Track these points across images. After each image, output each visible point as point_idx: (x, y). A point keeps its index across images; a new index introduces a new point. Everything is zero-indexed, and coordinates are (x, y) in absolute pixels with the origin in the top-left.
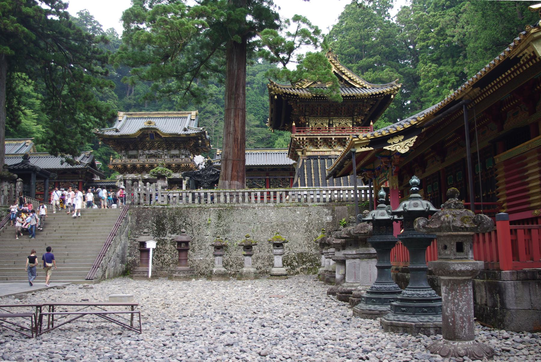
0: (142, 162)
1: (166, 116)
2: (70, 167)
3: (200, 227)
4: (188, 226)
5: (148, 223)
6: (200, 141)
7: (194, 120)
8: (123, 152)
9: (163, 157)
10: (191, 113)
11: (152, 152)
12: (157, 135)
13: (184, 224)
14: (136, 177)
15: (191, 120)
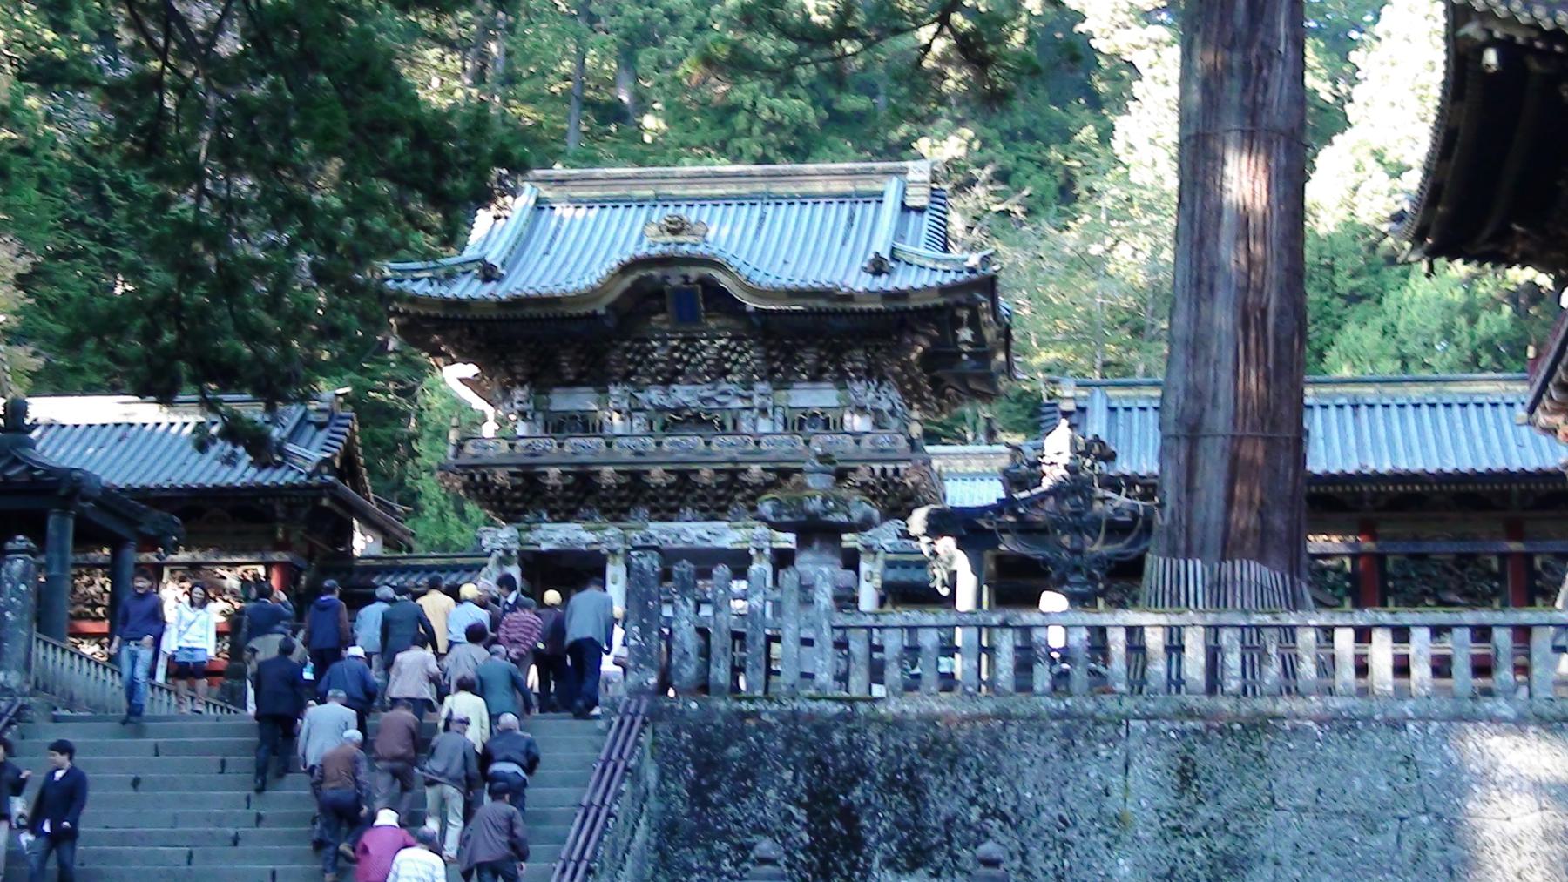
0: (627, 456)
1: (760, 187)
2: (243, 473)
3: (1073, 834)
4: (995, 824)
5: (762, 803)
6: (966, 334)
7: (920, 210)
9: (745, 426)
10: (902, 172)
11: (683, 394)
12: (717, 299)
13: (975, 814)
14: (589, 537)
15: (905, 208)
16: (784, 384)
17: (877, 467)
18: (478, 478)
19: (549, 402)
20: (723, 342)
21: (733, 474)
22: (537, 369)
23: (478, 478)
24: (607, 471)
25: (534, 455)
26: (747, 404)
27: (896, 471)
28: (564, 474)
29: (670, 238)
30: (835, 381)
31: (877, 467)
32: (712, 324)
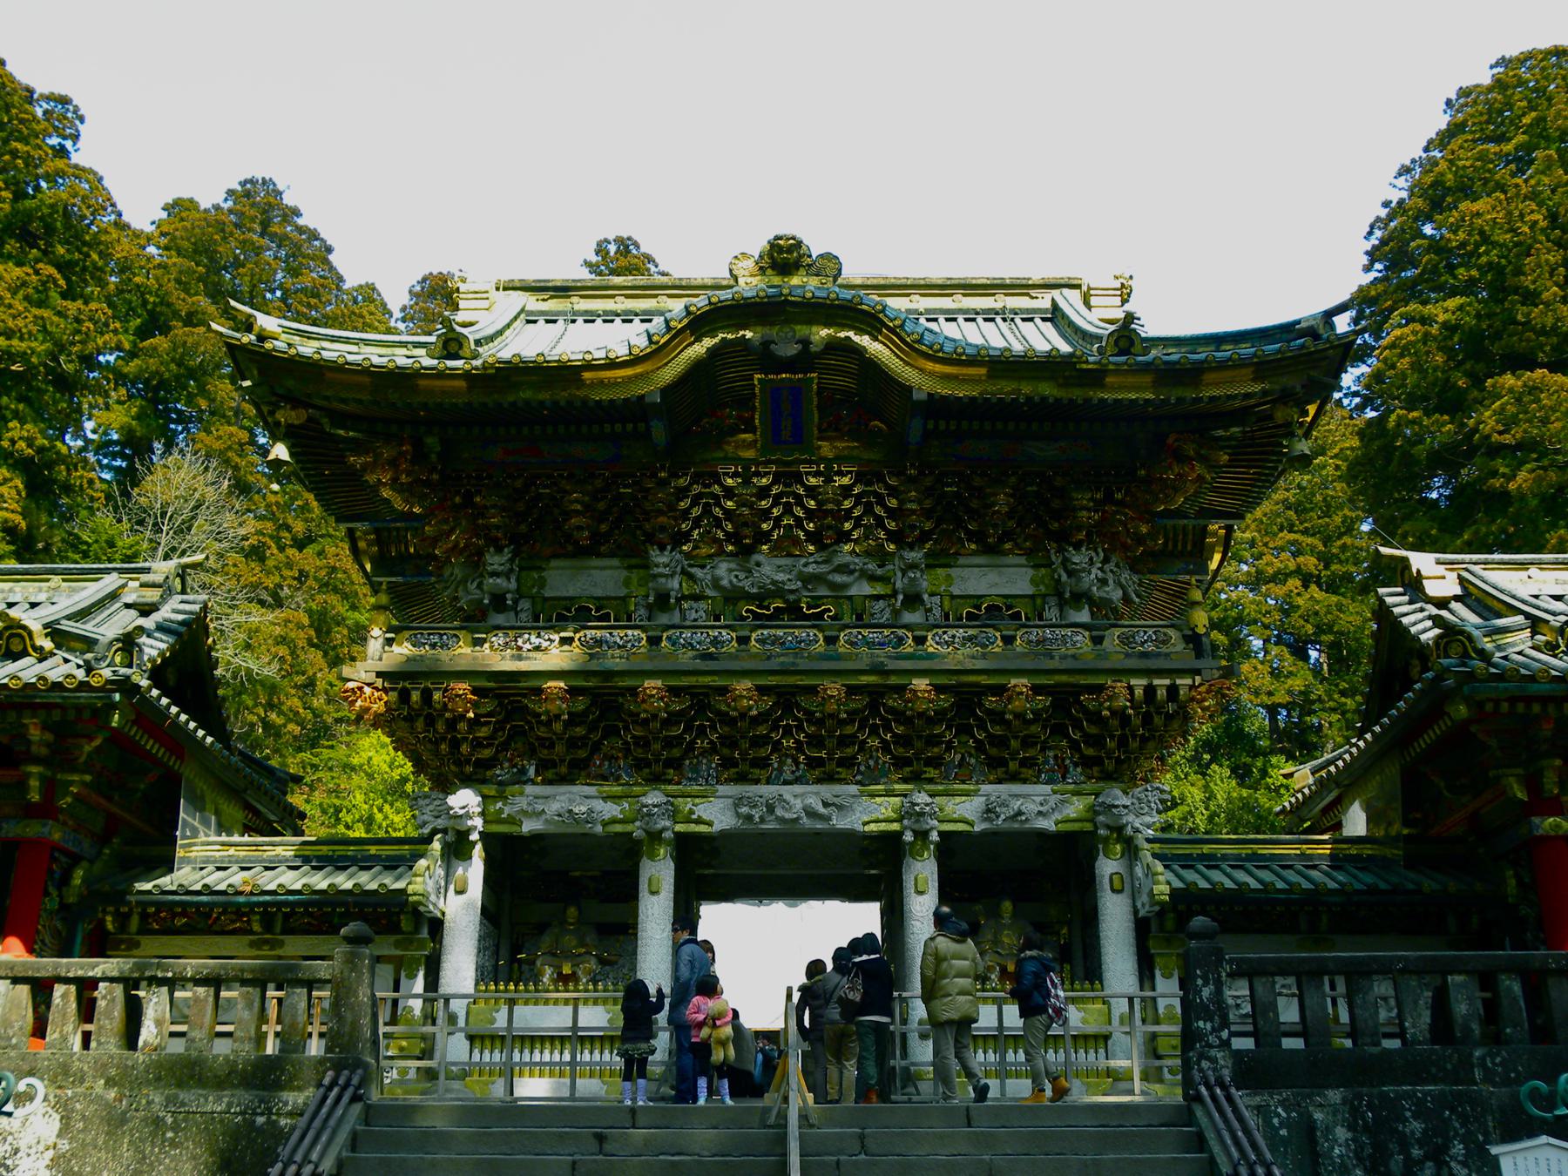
0: (685, 659)
8: (495, 561)
11: (770, 569)
14: (610, 810)
16: (940, 559)
17: (1139, 683)
18: (415, 696)
19: (542, 583)
20: (846, 481)
21: (875, 695)
22: (523, 528)
23: (415, 696)
24: (652, 685)
25: (520, 658)
26: (879, 589)
27: (1173, 690)
28: (573, 692)
29: (777, 280)
30: (1029, 553)
31: (1139, 683)
32: (826, 449)
